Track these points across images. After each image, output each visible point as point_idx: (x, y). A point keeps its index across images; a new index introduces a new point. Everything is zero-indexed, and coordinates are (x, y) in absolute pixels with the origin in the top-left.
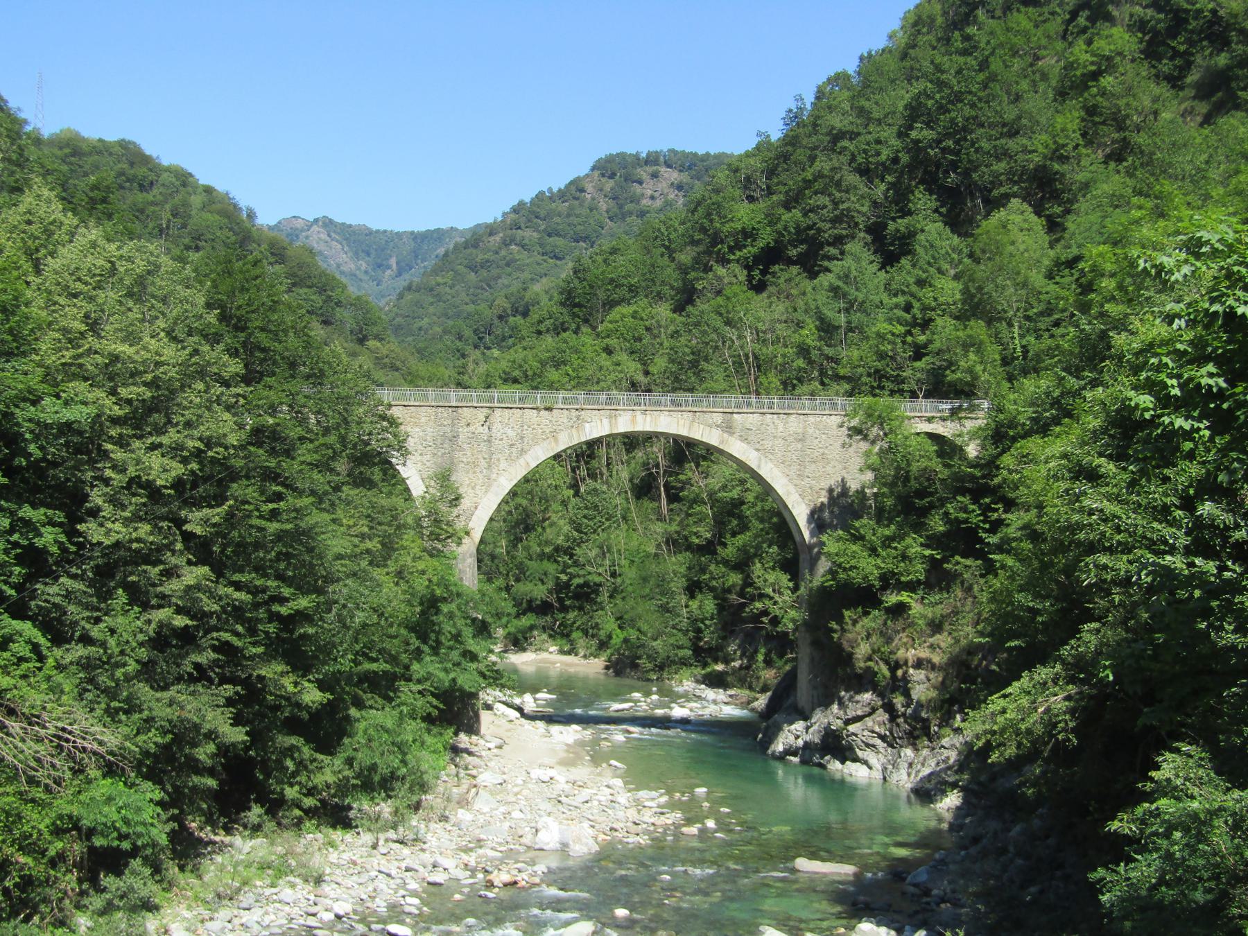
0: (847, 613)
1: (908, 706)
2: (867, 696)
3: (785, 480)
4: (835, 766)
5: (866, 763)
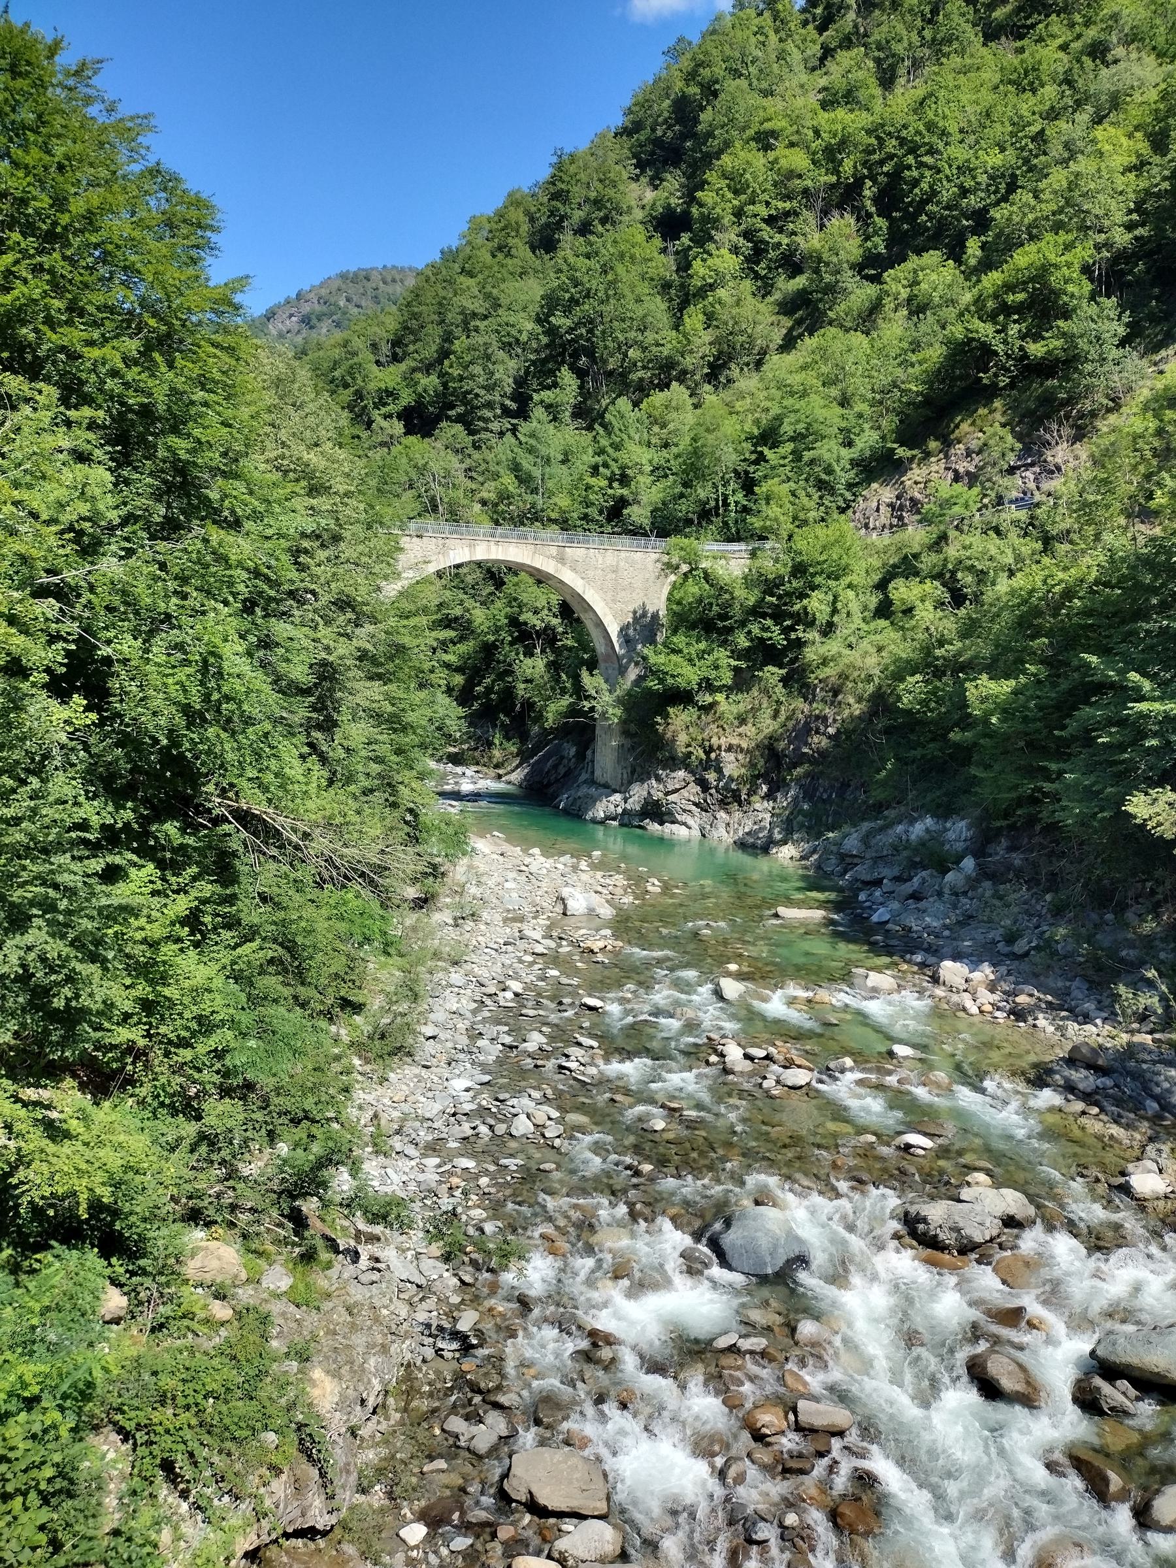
0: (671, 710)
1: (719, 780)
2: (681, 774)
3: (602, 604)
4: (654, 827)
5: (685, 824)
